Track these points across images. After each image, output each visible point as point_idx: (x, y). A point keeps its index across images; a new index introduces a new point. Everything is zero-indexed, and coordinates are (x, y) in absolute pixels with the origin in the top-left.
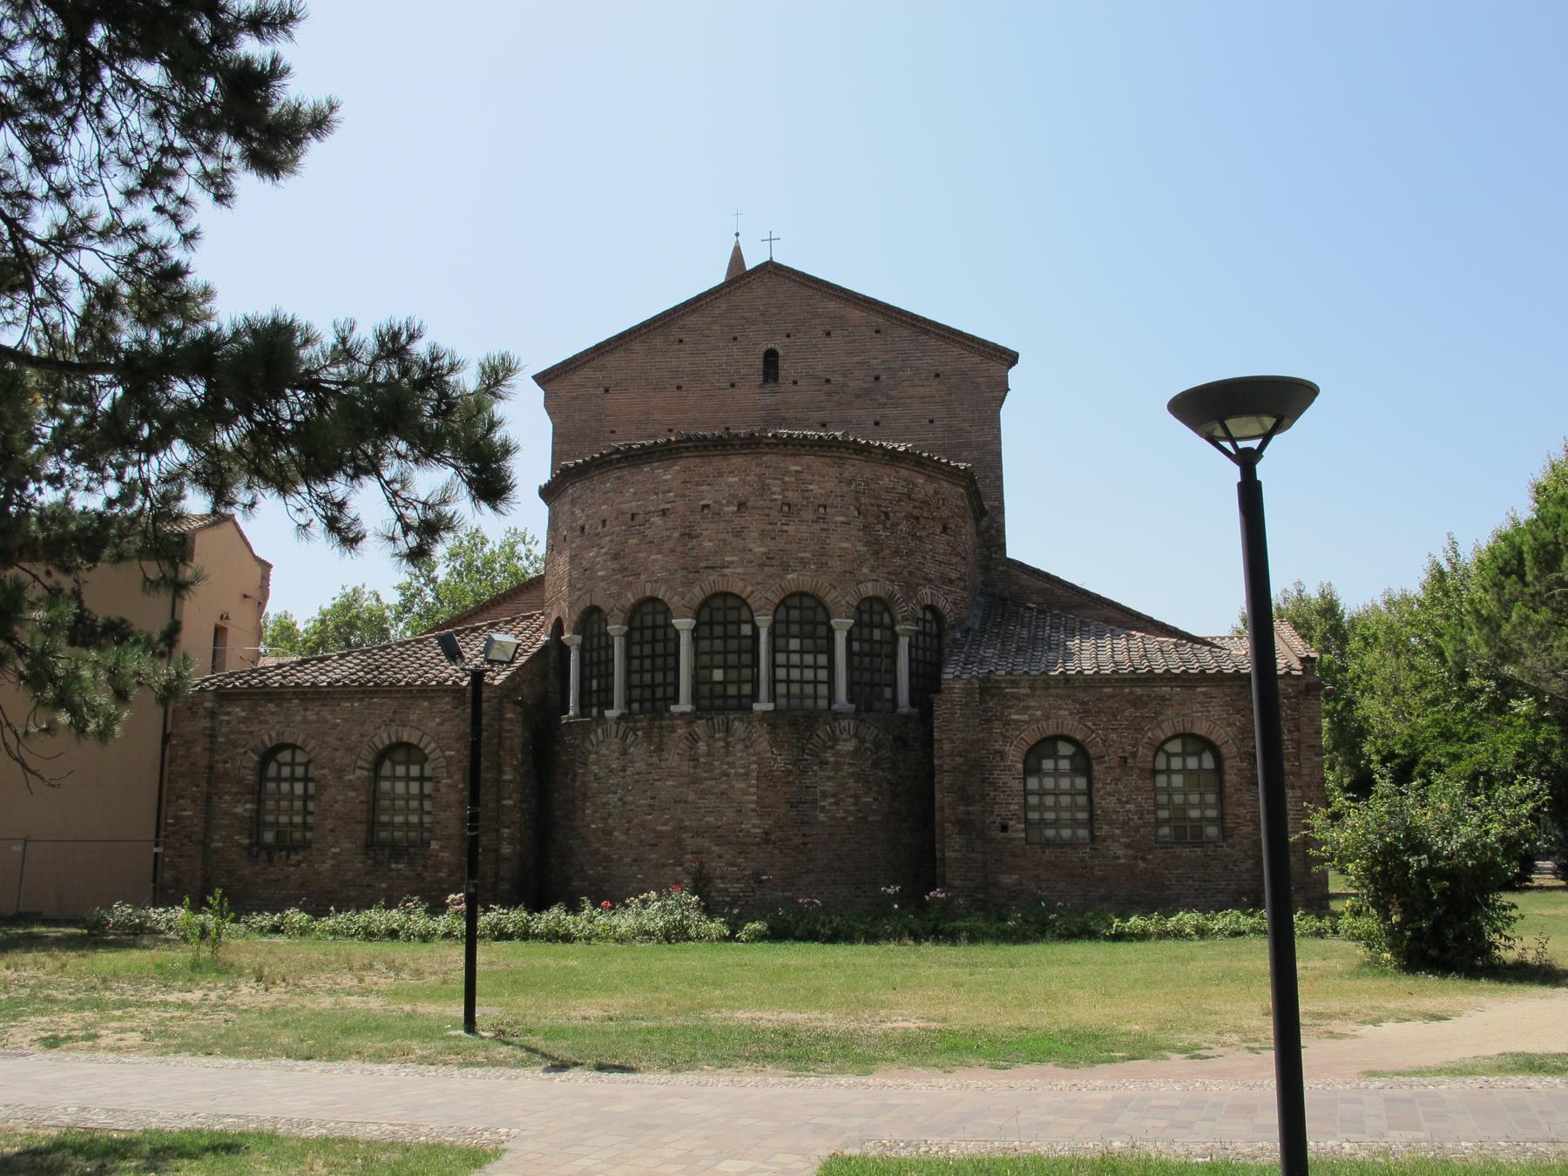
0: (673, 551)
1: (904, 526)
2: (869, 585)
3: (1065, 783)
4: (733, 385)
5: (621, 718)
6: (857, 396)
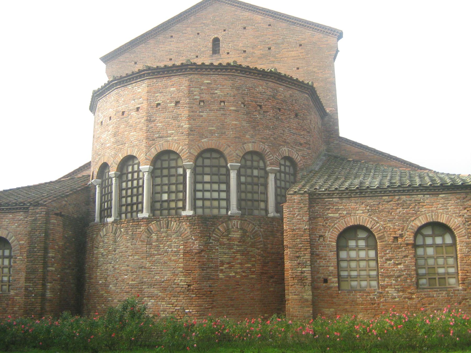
0: (141, 129)
1: (271, 113)
2: (250, 145)
3: (362, 254)
4: (197, 57)
5: (115, 222)
6: (259, 58)
